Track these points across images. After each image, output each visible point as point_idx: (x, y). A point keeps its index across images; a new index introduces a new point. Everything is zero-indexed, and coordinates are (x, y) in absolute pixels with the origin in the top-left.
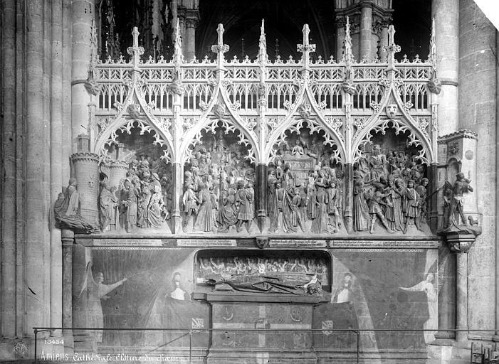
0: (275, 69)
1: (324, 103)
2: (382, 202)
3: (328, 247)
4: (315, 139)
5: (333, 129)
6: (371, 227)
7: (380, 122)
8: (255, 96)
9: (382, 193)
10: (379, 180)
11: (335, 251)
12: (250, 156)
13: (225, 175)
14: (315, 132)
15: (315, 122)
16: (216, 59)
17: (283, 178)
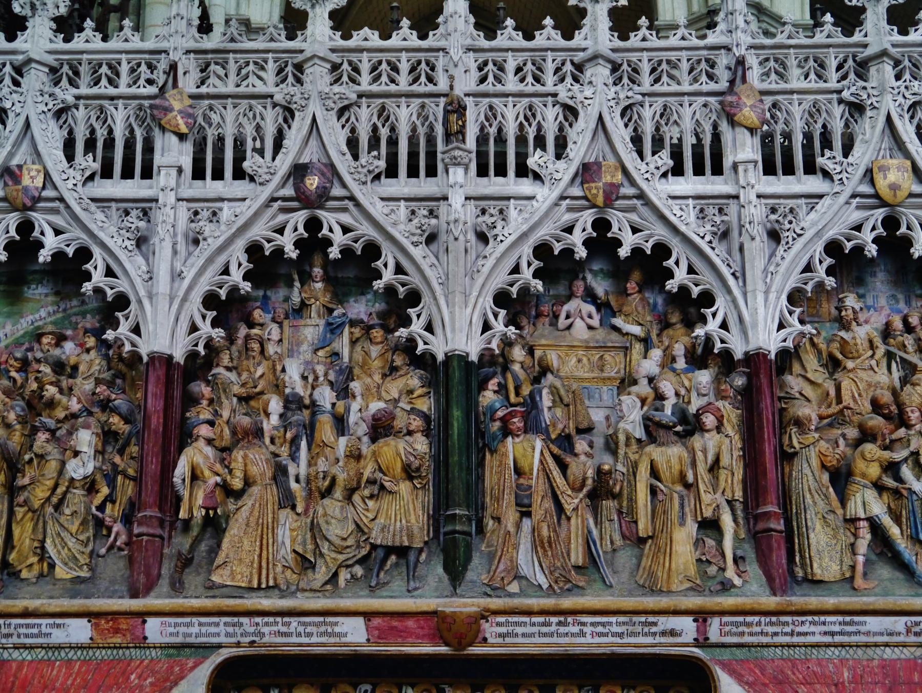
0: (499, 56)
1: (665, 160)
2: (890, 482)
3: (702, 642)
4: (636, 276)
5: (697, 240)
6: (853, 568)
7: (856, 216)
8: (431, 140)
9: (885, 448)
10: (869, 407)
11: (726, 655)
12: (417, 327)
13: (326, 396)
14: (637, 251)
15: (634, 217)
16: (303, 27)
17: (532, 403)
